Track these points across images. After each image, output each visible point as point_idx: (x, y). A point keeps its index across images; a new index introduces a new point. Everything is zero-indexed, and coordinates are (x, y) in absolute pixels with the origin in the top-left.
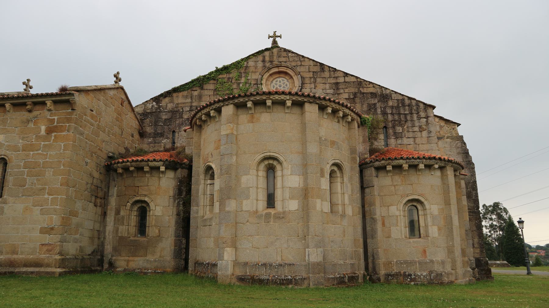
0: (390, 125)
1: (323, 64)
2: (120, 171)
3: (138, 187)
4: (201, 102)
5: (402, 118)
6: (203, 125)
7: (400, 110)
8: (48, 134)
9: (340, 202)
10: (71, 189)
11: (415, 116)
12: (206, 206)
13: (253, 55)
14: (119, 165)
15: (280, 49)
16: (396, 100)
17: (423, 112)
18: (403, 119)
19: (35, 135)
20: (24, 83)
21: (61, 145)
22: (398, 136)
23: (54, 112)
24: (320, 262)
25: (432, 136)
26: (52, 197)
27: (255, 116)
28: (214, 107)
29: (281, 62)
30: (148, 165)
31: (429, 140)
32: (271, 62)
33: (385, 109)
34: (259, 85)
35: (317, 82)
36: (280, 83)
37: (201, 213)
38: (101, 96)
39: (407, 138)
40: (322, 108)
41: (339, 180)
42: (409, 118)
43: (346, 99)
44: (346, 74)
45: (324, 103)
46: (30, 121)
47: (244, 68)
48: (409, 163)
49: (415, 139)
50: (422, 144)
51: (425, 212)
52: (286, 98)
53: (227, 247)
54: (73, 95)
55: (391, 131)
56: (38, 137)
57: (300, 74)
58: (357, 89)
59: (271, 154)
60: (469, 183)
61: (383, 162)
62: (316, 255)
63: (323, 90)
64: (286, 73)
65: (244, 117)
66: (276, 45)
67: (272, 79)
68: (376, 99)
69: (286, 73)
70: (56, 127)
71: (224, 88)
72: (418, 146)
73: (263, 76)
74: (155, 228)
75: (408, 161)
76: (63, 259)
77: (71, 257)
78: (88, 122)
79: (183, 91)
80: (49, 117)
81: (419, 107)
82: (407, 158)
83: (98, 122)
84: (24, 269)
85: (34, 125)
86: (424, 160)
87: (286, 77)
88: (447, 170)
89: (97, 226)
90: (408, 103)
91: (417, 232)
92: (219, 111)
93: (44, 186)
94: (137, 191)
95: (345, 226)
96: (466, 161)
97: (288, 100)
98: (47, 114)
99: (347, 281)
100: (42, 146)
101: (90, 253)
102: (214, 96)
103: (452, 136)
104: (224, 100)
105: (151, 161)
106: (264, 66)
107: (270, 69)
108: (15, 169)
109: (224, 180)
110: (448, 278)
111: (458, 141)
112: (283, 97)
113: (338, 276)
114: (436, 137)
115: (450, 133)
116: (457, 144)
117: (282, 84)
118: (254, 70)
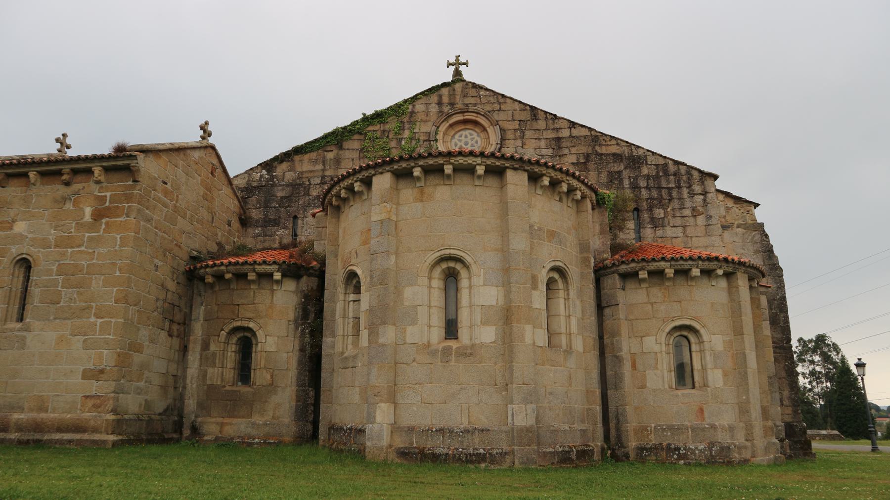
0: (645, 205)
1: (535, 107)
2: (209, 279)
3: (238, 305)
4: (339, 170)
5: (664, 195)
6: (342, 206)
7: (660, 181)
8: (95, 220)
9: (563, 330)
10: (131, 308)
11: (685, 191)
12: (348, 336)
13: (423, 93)
14: (207, 270)
15: (467, 84)
16: (654, 165)
17: (698, 185)
18: (665, 196)
19: (74, 223)
20: (57, 140)
21: (116, 238)
22: (656, 224)
23: (105, 184)
24: (532, 426)
25: (714, 223)
26: (101, 320)
27: (426, 190)
28: (360, 177)
29: (467, 105)
30: (254, 271)
31: (708, 231)
32: (452, 104)
33: (637, 179)
34: (432, 143)
35: (526, 137)
36: (466, 140)
37: (339, 348)
38: (179, 159)
40: (534, 178)
41: (562, 294)
42: (675, 194)
43: (573, 164)
44: (573, 125)
46: (67, 200)
47: (409, 115)
48: (676, 267)
49: (684, 229)
50: (696, 236)
51: (702, 347)
52: (476, 162)
53: (381, 401)
54: (135, 157)
55: (646, 216)
56: (80, 225)
57: (498, 124)
58: (590, 148)
59: (452, 252)
60: (774, 300)
61: (633, 265)
63: (535, 149)
64: (476, 123)
65: (408, 192)
66: (460, 77)
67: (453, 132)
68: (622, 164)
69: (476, 123)
70: (108, 208)
71: (376, 147)
72: (690, 241)
73: (438, 127)
74: (265, 371)
75: (673, 263)
76: (118, 421)
77: (131, 416)
78: (159, 200)
79: (310, 152)
80: (97, 193)
81: (692, 176)
82: (672, 259)
83: (174, 202)
84: (58, 436)
85: (74, 206)
86: (700, 262)
87: (476, 130)
88: (737, 279)
89: (173, 369)
90: (674, 170)
91: (688, 380)
92: (368, 183)
93: (89, 304)
94: (237, 312)
95: (571, 368)
96: (769, 265)
97: (478, 164)
98: (95, 189)
99: (574, 457)
100: (86, 239)
101: (161, 411)
102: (360, 159)
103: (745, 224)
104: (377, 166)
105: (260, 264)
106: (441, 112)
107: (449, 116)
108: (45, 276)
109: (377, 295)
110: (740, 454)
111: (756, 232)
112: (470, 160)
113: (560, 450)
114: (719, 225)
115: (743, 220)
116: (754, 236)
117: (470, 141)
118: (424, 118)
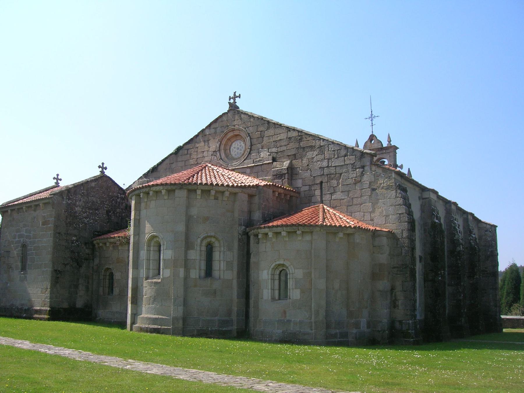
45: (190, 187)
62: (177, 312)
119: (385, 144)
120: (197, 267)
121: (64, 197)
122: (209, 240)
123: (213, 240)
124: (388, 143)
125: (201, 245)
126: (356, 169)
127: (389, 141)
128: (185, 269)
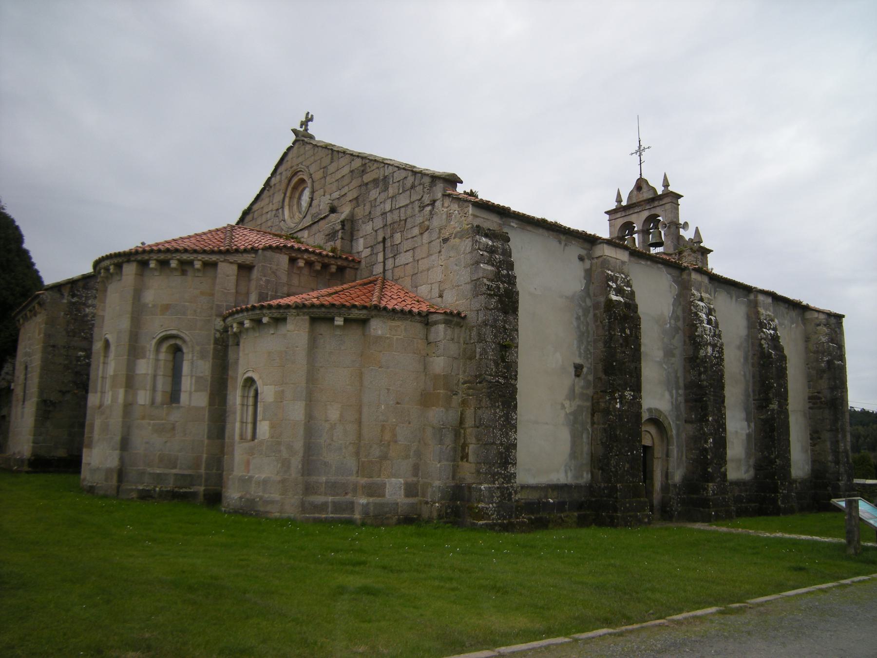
39: (405, 252)
45: (139, 258)
50: (422, 258)
55: (388, 244)
67: (297, 195)
111: (469, 239)
119: (660, 192)
120: (149, 387)
121: (65, 294)
122: (172, 342)
123: (179, 342)
124: (663, 188)
125: (158, 350)
126: (424, 207)
127: (666, 184)
128: (126, 392)
